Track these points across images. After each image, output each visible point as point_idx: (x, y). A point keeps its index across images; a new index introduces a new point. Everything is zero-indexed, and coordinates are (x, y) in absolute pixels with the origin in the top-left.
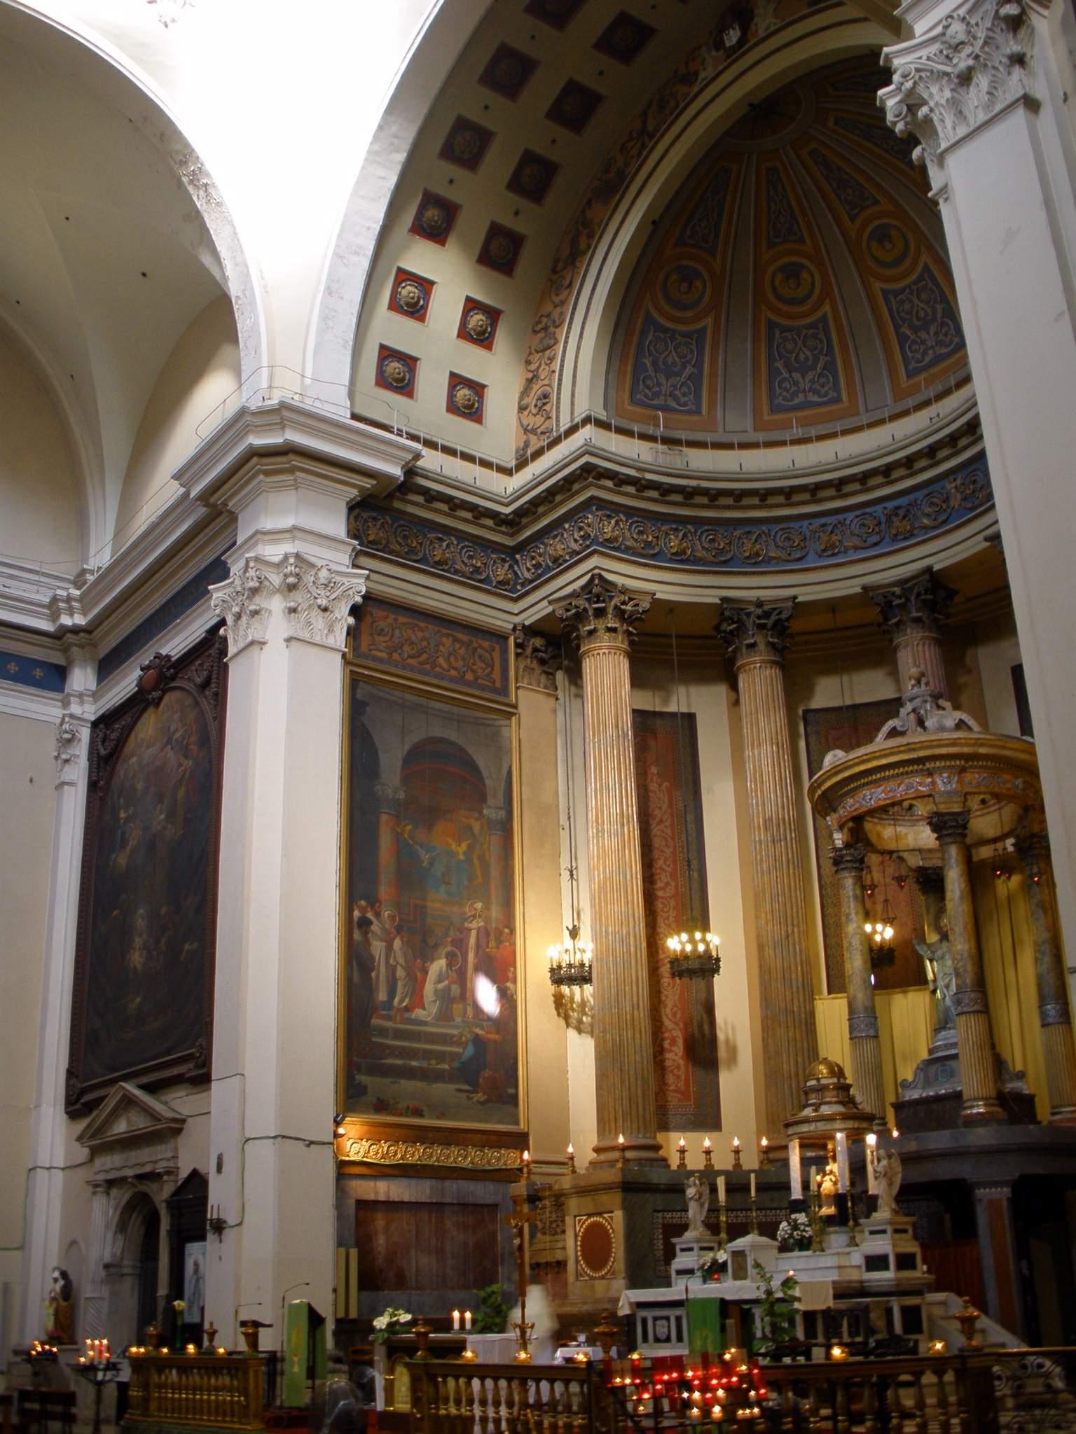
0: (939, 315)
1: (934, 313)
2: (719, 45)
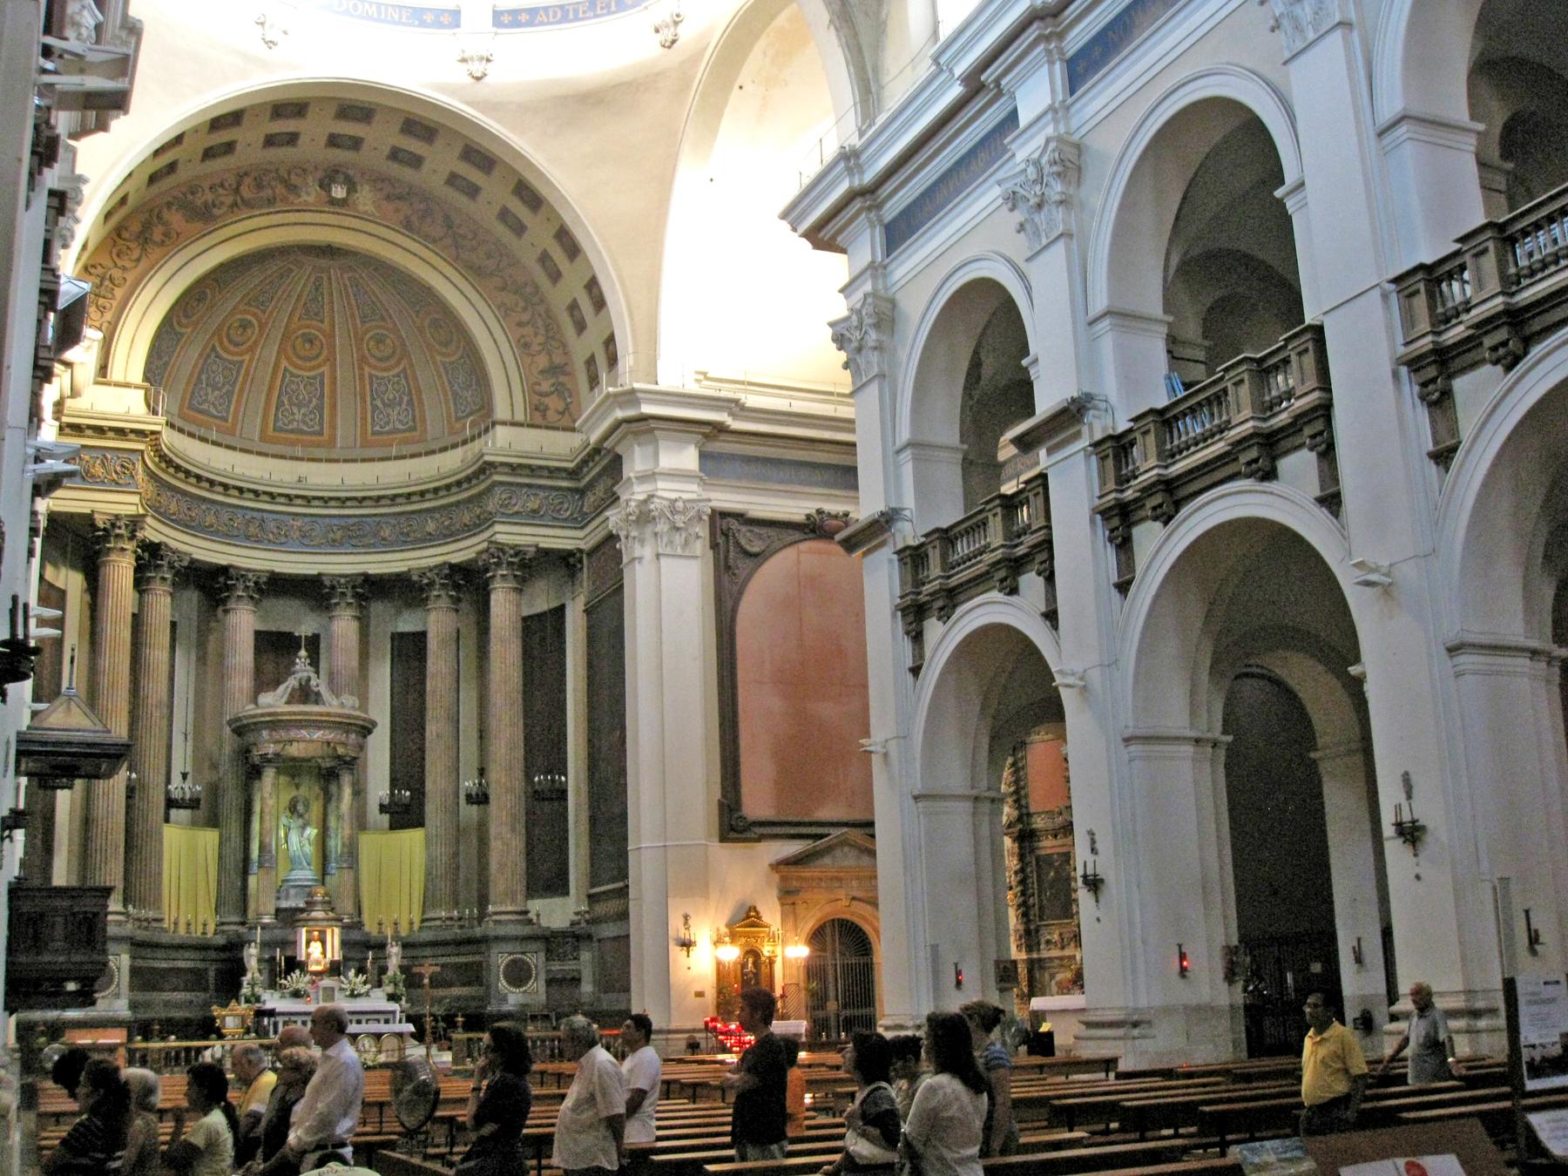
0: (312, 406)
1: (310, 401)
2: (325, 185)
